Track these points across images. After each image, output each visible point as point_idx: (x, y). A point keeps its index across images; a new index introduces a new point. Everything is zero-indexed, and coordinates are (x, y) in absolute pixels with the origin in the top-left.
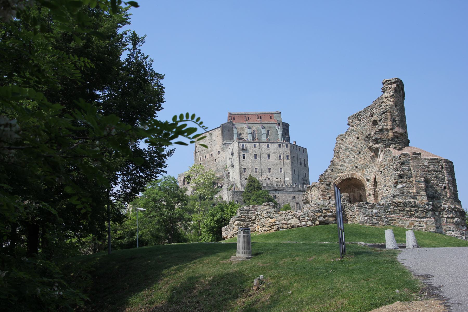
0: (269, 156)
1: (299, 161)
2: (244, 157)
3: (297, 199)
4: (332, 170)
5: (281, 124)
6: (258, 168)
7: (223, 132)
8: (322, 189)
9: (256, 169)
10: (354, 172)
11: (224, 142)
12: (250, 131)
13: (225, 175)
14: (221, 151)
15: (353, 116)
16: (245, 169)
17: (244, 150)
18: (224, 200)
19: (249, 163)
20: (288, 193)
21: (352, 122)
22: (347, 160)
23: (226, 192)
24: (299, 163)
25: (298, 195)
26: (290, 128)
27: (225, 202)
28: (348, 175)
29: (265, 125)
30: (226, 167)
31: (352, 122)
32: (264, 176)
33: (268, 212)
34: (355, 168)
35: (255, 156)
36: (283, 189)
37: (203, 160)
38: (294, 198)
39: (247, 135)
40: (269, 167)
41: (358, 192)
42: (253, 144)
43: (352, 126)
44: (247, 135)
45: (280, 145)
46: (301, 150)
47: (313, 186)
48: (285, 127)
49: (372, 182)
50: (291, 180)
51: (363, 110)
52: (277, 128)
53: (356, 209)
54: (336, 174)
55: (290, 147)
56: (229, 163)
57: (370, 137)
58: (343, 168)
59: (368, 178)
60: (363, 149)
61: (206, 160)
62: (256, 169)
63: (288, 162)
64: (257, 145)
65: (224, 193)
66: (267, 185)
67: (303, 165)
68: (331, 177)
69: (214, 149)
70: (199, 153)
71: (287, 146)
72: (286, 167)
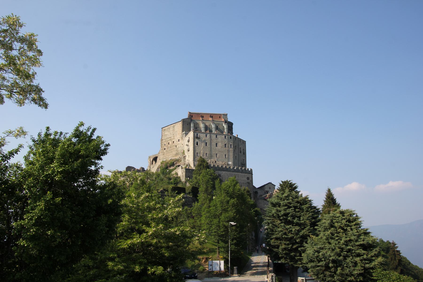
0: (217, 144)
2: (197, 144)
9: (206, 154)
13: (182, 157)
14: (180, 139)
26: (234, 126)
29: (215, 122)
30: (184, 152)
37: (167, 146)
40: (217, 152)
45: (225, 137)
48: (230, 125)
55: (234, 138)
56: (186, 148)
61: (169, 146)
62: (206, 154)
63: (231, 149)
64: (208, 135)
65: (179, 170)
66: (214, 166)
67: (242, 153)
69: (175, 138)
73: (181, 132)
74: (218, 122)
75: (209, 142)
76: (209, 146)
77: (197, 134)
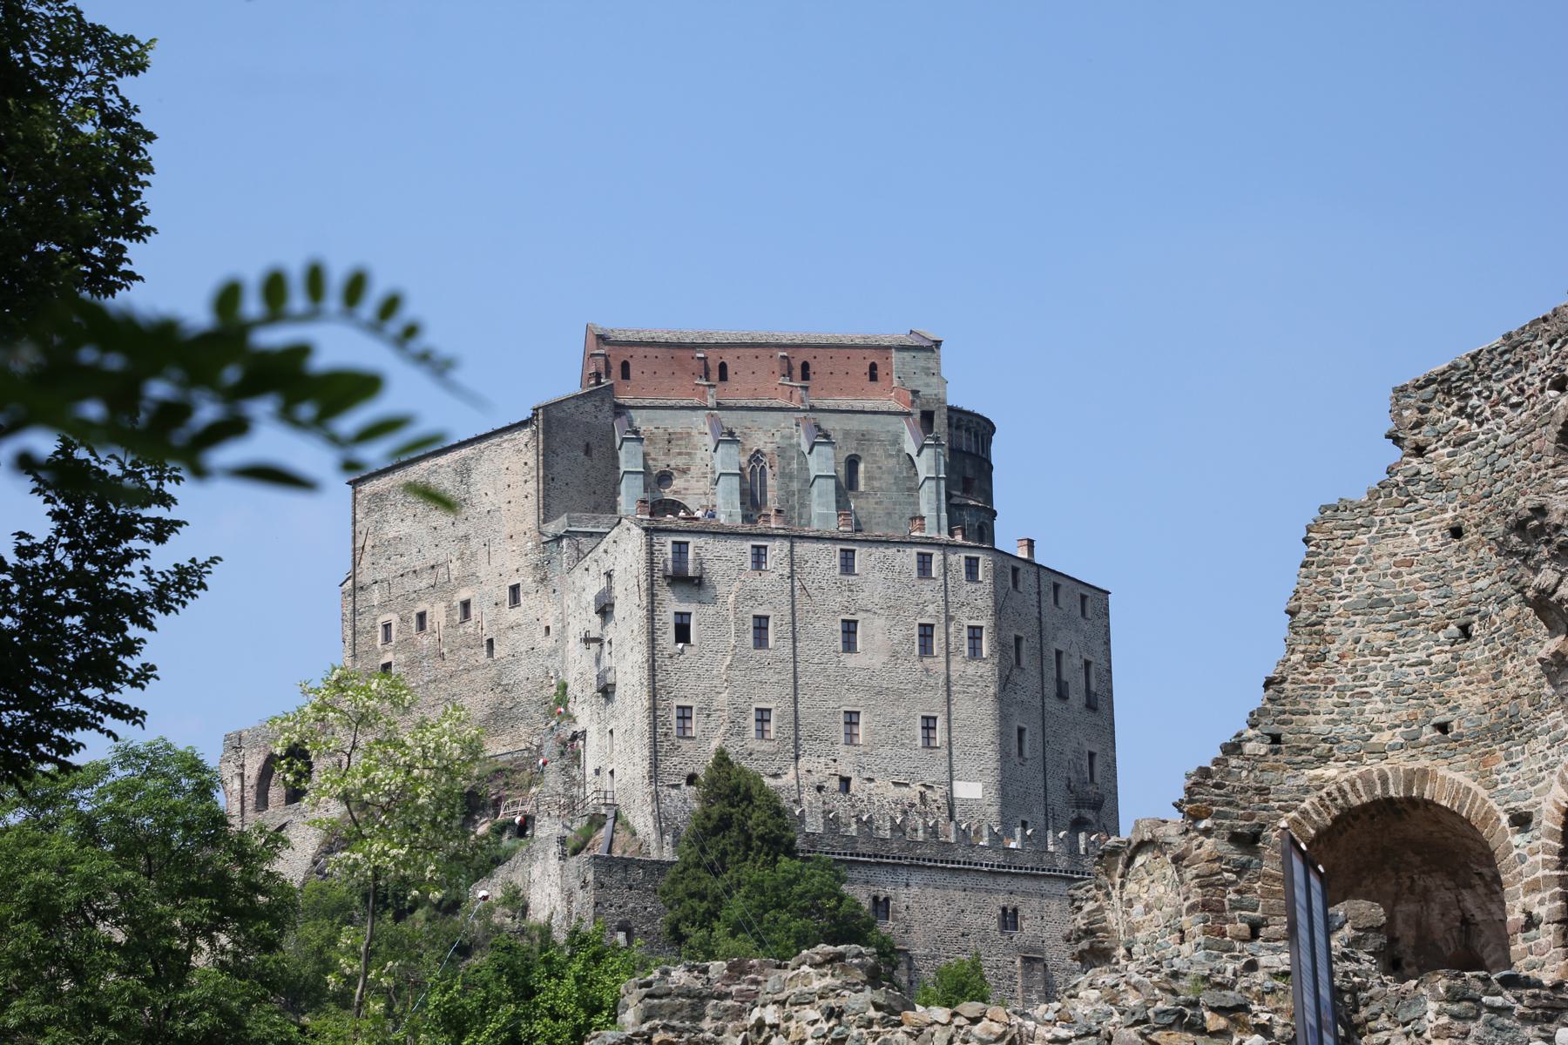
0: (849, 628)
1: (1051, 674)
2: (682, 633)
3: (1028, 928)
4: (1276, 739)
5: (940, 422)
6: (778, 707)
7: (548, 457)
8: (1202, 867)
9: (763, 716)
10: (1427, 763)
11: (553, 528)
12: (730, 459)
13: (551, 748)
14: (527, 582)
15: (1429, 381)
16: (684, 713)
17: (686, 581)
18: (538, 915)
19: (714, 669)
20: (969, 881)
21: (1418, 425)
22: (1378, 678)
23: (553, 863)
24: (1051, 688)
25: (1035, 902)
26: (1000, 451)
27: (546, 931)
28: (1384, 779)
31: (1418, 425)
32: (816, 766)
33: (831, 1013)
34: (1428, 733)
35: (761, 624)
36: (939, 857)
38: (1009, 919)
39: (709, 486)
41: (1449, 896)
42: (747, 545)
43: (1419, 451)
44: (709, 486)
46: (1068, 600)
47: (1142, 846)
48: (966, 442)
49: (1551, 834)
50: (993, 796)
51: (1496, 340)
52: (910, 447)
53: (1432, 1013)
54: (1299, 766)
55: (997, 574)
57: (1541, 529)
58: (1351, 729)
59: (1522, 806)
60: (1492, 608)
61: (425, 641)
62: (763, 716)
63: (978, 677)
64: (776, 551)
65: (536, 871)
66: (833, 823)
67: (1077, 698)
68: (1262, 791)
69: (483, 571)
70: (376, 596)
71: (972, 564)
72: (963, 707)
73: (531, 520)
74: (856, 424)
75: (787, 609)
76: (788, 651)
77: (681, 548)
